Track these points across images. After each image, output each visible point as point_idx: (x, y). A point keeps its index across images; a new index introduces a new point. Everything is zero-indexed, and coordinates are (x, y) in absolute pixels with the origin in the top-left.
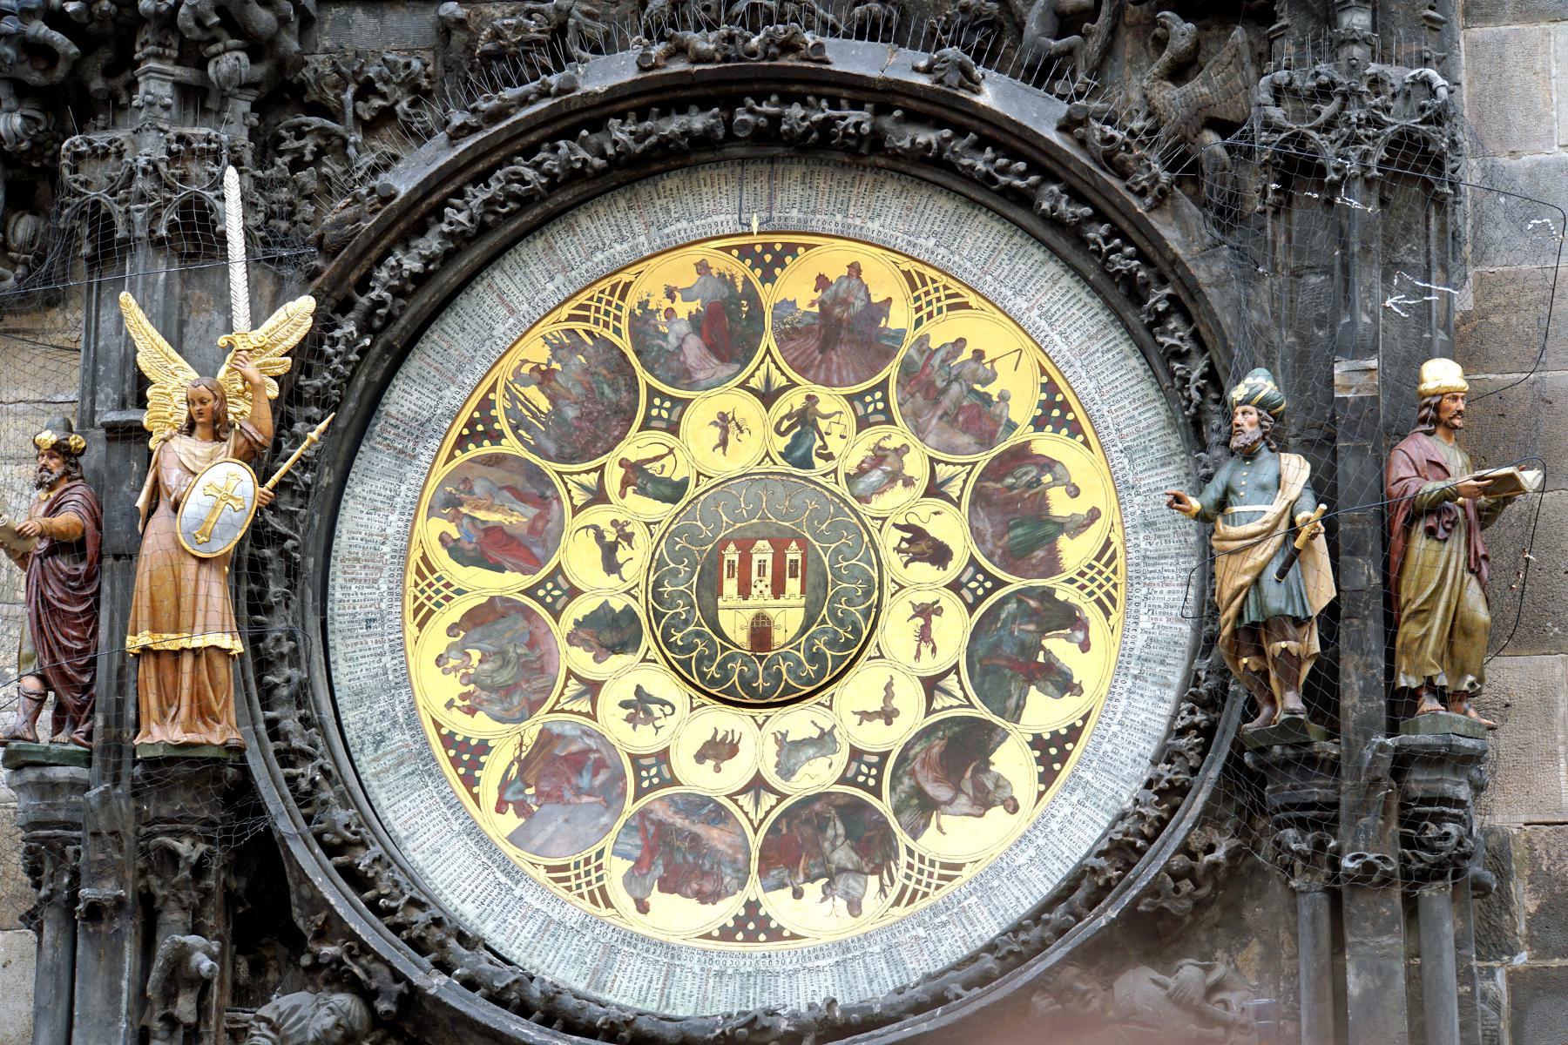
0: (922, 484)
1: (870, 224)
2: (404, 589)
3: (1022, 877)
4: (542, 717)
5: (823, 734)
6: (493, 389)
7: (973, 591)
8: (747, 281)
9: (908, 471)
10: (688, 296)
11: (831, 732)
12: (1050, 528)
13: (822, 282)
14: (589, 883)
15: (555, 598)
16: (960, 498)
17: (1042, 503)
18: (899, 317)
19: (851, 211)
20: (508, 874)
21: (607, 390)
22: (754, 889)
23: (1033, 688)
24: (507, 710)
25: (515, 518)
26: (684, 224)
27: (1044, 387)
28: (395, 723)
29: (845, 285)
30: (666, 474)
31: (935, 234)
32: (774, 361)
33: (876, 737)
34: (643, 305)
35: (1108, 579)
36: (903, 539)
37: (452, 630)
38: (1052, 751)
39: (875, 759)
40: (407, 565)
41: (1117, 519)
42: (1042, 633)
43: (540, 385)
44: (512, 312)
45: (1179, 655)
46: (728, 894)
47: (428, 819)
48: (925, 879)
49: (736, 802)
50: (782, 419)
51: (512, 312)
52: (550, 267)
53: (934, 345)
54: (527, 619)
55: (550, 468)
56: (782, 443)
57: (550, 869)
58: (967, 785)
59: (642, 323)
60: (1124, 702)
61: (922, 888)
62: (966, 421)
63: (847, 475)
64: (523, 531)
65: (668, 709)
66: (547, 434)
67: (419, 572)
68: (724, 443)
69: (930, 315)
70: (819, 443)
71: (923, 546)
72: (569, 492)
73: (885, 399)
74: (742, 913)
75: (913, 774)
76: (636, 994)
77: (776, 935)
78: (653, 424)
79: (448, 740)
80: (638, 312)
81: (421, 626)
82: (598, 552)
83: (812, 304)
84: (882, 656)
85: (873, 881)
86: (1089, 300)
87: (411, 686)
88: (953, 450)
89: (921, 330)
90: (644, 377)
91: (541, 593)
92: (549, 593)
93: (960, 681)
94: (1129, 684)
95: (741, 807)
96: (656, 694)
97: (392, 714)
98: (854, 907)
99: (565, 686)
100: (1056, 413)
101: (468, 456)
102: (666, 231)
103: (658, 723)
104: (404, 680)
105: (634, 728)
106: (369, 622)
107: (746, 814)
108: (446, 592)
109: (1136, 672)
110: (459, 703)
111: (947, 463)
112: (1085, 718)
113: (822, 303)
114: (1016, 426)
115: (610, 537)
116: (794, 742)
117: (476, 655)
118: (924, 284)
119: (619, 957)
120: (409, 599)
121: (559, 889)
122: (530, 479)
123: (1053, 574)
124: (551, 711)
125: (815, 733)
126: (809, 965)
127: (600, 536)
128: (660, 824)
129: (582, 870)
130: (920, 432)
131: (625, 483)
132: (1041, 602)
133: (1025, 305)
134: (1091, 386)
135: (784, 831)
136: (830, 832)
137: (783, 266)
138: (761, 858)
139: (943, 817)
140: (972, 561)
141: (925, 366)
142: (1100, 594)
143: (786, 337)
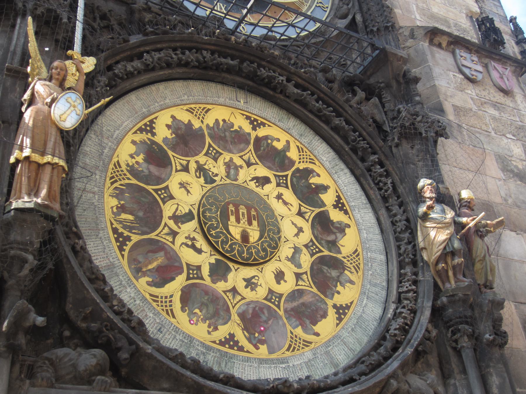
0: (244, 165)
4: (234, 312)
6: (112, 224)
7: (283, 183)
8: (149, 139)
9: (238, 164)
12: (282, 153)
16: (256, 161)
17: (276, 149)
18: (196, 124)
20: (282, 363)
21: (143, 199)
23: (320, 195)
24: (223, 319)
26: (117, 132)
28: (204, 354)
29: (174, 123)
30: (184, 213)
32: (178, 158)
34: (128, 165)
36: (255, 183)
37: (183, 309)
38: (339, 205)
39: (311, 244)
42: (307, 180)
47: (246, 372)
50: (195, 173)
51: (94, 193)
53: (211, 125)
54: (197, 287)
55: (153, 236)
56: (202, 180)
57: (288, 350)
58: (335, 230)
60: (340, 181)
65: (257, 278)
67: (155, 301)
68: (188, 192)
70: (211, 173)
71: (261, 181)
72: (165, 239)
75: (322, 239)
77: (348, 307)
79: (221, 343)
80: (128, 168)
82: (191, 251)
83: (172, 135)
84: (283, 217)
85: (346, 272)
88: (242, 151)
89: (205, 124)
90: (150, 188)
93: (305, 207)
95: (302, 285)
96: (249, 277)
97: (200, 352)
98: (352, 282)
99: (228, 297)
102: (114, 137)
103: (259, 284)
105: (256, 291)
107: (305, 286)
108: (168, 300)
110: (210, 330)
111: (244, 155)
113: (174, 132)
115: (190, 243)
117: (197, 311)
118: (194, 110)
119: (331, 353)
120: (161, 312)
124: (233, 307)
125: (293, 250)
126: (363, 305)
127: (187, 245)
128: (292, 309)
130: (230, 151)
131: (176, 223)
133: (223, 100)
136: (325, 271)
143: (173, 149)
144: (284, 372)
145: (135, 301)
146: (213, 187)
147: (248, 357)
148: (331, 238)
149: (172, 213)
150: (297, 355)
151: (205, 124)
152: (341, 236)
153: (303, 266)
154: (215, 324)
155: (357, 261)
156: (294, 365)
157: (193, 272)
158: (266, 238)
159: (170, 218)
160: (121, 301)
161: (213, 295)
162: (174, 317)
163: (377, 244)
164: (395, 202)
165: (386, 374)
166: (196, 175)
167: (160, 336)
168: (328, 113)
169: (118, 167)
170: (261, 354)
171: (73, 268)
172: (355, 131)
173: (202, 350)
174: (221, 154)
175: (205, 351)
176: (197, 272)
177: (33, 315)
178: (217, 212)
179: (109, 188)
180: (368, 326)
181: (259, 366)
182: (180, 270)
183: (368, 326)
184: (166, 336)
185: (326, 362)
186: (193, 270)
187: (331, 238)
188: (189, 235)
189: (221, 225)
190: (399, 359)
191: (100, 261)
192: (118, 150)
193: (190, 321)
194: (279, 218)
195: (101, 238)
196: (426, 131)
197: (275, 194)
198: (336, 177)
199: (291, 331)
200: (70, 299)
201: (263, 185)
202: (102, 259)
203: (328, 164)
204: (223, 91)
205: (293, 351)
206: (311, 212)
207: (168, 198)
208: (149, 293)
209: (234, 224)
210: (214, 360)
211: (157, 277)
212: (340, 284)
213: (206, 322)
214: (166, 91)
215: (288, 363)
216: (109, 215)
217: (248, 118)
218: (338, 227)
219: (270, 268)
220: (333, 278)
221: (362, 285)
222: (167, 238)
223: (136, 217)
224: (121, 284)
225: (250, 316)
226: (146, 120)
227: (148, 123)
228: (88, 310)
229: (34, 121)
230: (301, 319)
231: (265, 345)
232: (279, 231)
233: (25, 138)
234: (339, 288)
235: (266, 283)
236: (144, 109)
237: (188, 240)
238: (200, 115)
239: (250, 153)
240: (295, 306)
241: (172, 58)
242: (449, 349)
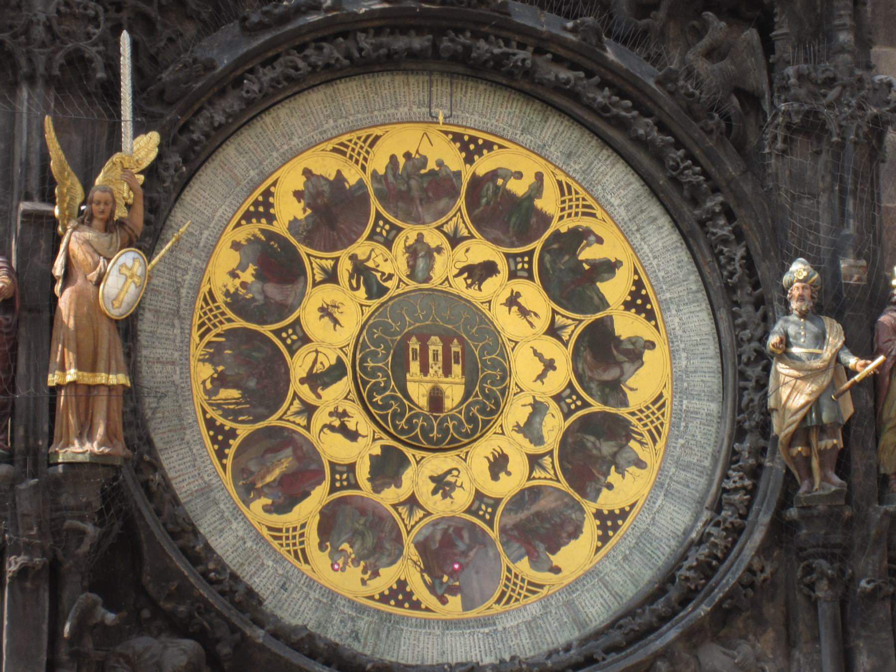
0: (446, 244)
1: (293, 143)
2: (280, 554)
3: (692, 370)
6: (205, 412)
7: (523, 269)
8: (263, 231)
9: (433, 245)
10: (243, 267)
12: (526, 204)
13: (298, 195)
16: (470, 232)
18: (352, 176)
19: (277, 145)
20: (485, 625)
21: (255, 354)
22: (590, 507)
23: (598, 284)
24: (389, 555)
25: (284, 464)
26: (206, 233)
28: (353, 619)
29: (310, 185)
30: (327, 365)
31: (328, 116)
32: (316, 257)
34: (227, 294)
35: (577, 199)
36: (465, 279)
37: (322, 547)
38: (638, 302)
39: (568, 391)
40: (266, 541)
41: (552, 167)
42: (574, 255)
44: (173, 363)
47: (421, 645)
48: (653, 418)
49: (534, 478)
51: (173, 363)
52: (167, 321)
53: (381, 171)
55: (272, 421)
56: (362, 293)
57: (498, 601)
58: (621, 358)
59: (237, 304)
60: (645, 247)
65: (455, 473)
67: (276, 538)
68: (336, 322)
69: (365, 159)
70: (378, 275)
71: (478, 272)
72: (294, 422)
73: (386, 222)
74: (598, 522)
75: (591, 379)
76: (602, 608)
77: (624, 514)
79: (384, 599)
80: (229, 300)
81: (306, 561)
82: (339, 437)
83: (305, 211)
84: (517, 343)
85: (633, 444)
87: (339, 594)
88: (443, 213)
89: (369, 171)
90: (266, 330)
91: (338, 484)
92: (341, 480)
93: (563, 316)
94: (638, 236)
95: (540, 478)
96: (440, 472)
98: (640, 464)
99: (400, 514)
100: (472, 147)
101: (231, 457)
102: (201, 245)
103: (458, 484)
104: (333, 596)
105: (451, 497)
106: (283, 587)
107: (545, 478)
108: (297, 533)
109: (636, 228)
110: (366, 577)
111: (447, 222)
112: (636, 272)
113: (308, 205)
115: (337, 423)
116: (526, 424)
117: (345, 546)
118: (347, 147)
119: (577, 603)
120: (286, 555)
121: (513, 605)
124: (408, 533)
125: (529, 409)
126: (655, 510)
127: (332, 428)
128: (516, 526)
129: (511, 586)
130: (418, 220)
131: (313, 389)
133: (406, 109)
134: (476, 117)
135: (570, 467)
136: (589, 445)
139: (627, 383)
141: (388, 187)
142: (580, 210)
143: (309, 241)
144: (486, 641)
145: (245, 543)
146: (382, 304)
147: (425, 619)
148: (611, 374)
149: (307, 370)
150: (513, 610)
151: (369, 171)
152: (633, 368)
153: (546, 440)
154: (375, 566)
155: (658, 419)
156: (504, 629)
158: (477, 395)
159: (302, 381)
160: (220, 561)
161: (374, 514)
162: (306, 561)
163: (707, 379)
164: (747, 299)
165: (649, 652)
167: (285, 596)
168: (624, 113)
169: (210, 302)
170: (449, 612)
171: (148, 526)
172: (678, 145)
173: (350, 612)
174: (400, 229)
175: (354, 614)
176: (348, 477)
177: (101, 610)
178: (387, 358)
179: (198, 345)
180: (657, 548)
181: (443, 634)
182: (317, 477)
183: (657, 548)
184: (293, 595)
185: (565, 620)
186: (341, 474)
187: (611, 374)
188: (337, 408)
189: (393, 383)
190: (680, 625)
191: (189, 484)
192: (209, 268)
193: (332, 565)
194: (509, 346)
195: (188, 443)
196: (841, 126)
197: (507, 294)
198: (637, 239)
199: (508, 567)
200: (147, 568)
201: (481, 280)
202: (192, 480)
203: (623, 213)
204: (406, 89)
206: (575, 325)
207: (299, 343)
208: (267, 526)
209: (417, 378)
210: (368, 628)
211: (280, 494)
212: (617, 469)
213: (359, 564)
214: (293, 119)
215: (495, 624)
216: (199, 396)
217: (457, 137)
218: (628, 350)
219: (482, 451)
220: (603, 458)
221: (660, 469)
224: (222, 517)
225: (437, 545)
226: (257, 194)
227: (261, 199)
228: (173, 585)
229: (76, 317)
230: (530, 544)
231: (459, 596)
232: (506, 374)
233: (66, 350)
234: (613, 477)
235: (472, 480)
237: (334, 418)
238: (359, 154)
239: (458, 217)
240: (521, 520)
241: (297, 69)
242: (799, 597)
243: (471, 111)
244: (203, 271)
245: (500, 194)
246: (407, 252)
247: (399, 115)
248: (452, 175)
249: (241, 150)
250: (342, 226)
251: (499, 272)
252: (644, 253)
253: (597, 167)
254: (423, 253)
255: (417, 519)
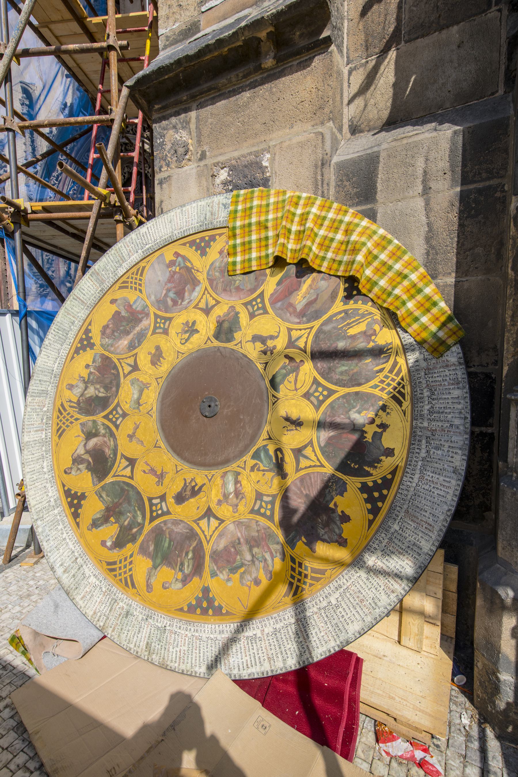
3: (40, 460)
4: (204, 283)
5: (139, 405)
8: (369, 474)
10: (377, 436)
11: (138, 408)
12: (158, 561)
13: (345, 518)
14: (131, 283)
15: (253, 306)
16: (198, 524)
17: (170, 564)
23: (103, 508)
26: (423, 454)
27: (220, 608)
29: (337, 530)
30: (286, 382)
33: (126, 427)
36: (196, 485)
43: (364, 333)
45: (72, 586)
46: (102, 338)
47: (184, 220)
49: (133, 356)
57: (144, 268)
58: (87, 457)
61: (61, 417)
62: (229, 552)
63: (238, 474)
64: (292, 301)
66: (335, 328)
71: (188, 493)
72: (300, 330)
73: (264, 515)
74: (92, 341)
75: (104, 436)
76: (83, 287)
77: (77, 351)
78: (314, 386)
82: (265, 334)
83: (335, 505)
85: (75, 399)
86: (249, 671)
88: (220, 536)
90: (342, 391)
91: (259, 300)
92: (257, 304)
94: (76, 554)
98: (71, 387)
99: (214, 299)
100: (205, 605)
102: (424, 441)
103: (180, 335)
105: (183, 324)
109: (78, 560)
113: (334, 511)
114: (212, 577)
119: (98, 285)
121: (134, 269)
122: (316, 312)
123: (140, 548)
124: (206, 289)
127: (272, 338)
128: (140, 320)
130: (239, 524)
132: (133, 535)
133: (266, 630)
134: (204, 636)
135: (112, 371)
136: (102, 390)
137: (367, 501)
138: (107, 358)
139: (81, 439)
140: (168, 513)
141: (269, 548)
155: (61, 421)
157: (258, 307)
163: (30, 457)
166: (282, 452)
169: (397, 395)
174: (252, 511)
176: (253, 309)
181: (172, 232)
192: (408, 424)
197: (166, 481)
203: (87, 570)
205: (138, 269)
210: (218, 214)
214: (371, 595)
215: (143, 252)
222: (299, 333)
223: (345, 337)
226: (385, 507)
227: (380, 504)
236: (397, 528)
237: (271, 346)
240: (138, 326)
243: (210, 641)
244: (413, 418)
245: (178, 564)
246: (243, 493)
247: (272, 623)
248: (218, 572)
249: (415, 548)
250: (300, 501)
251: (173, 497)
252: (72, 541)
253: (106, 608)
254: (231, 497)
255: (202, 300)
